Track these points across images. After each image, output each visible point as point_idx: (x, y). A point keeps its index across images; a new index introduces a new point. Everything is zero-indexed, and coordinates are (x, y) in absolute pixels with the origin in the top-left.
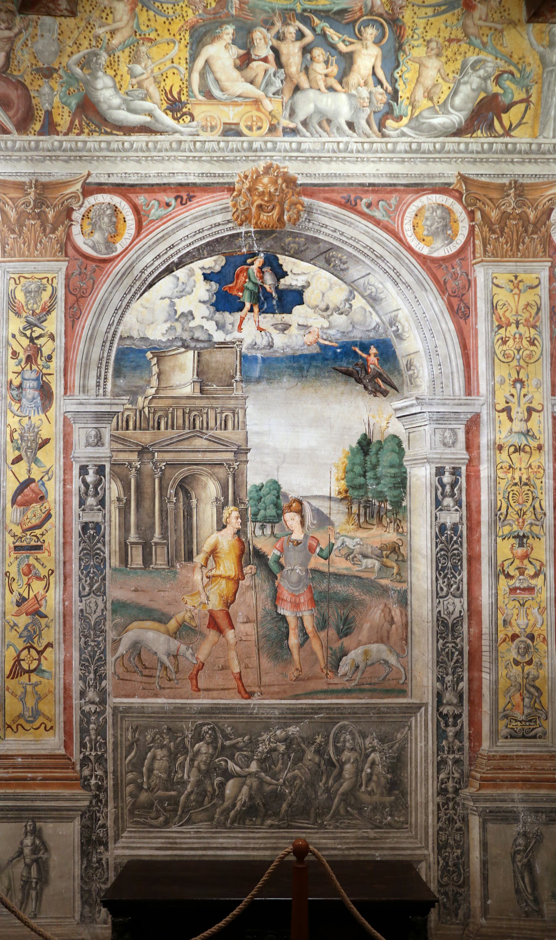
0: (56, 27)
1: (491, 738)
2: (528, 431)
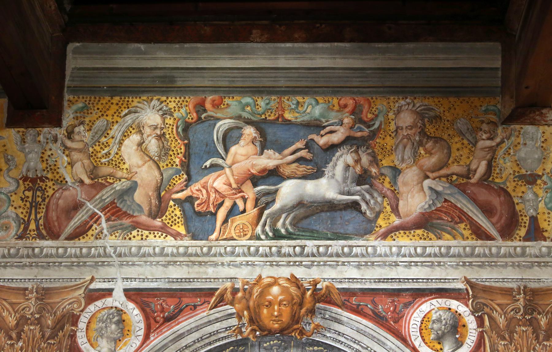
0: (539, 135)
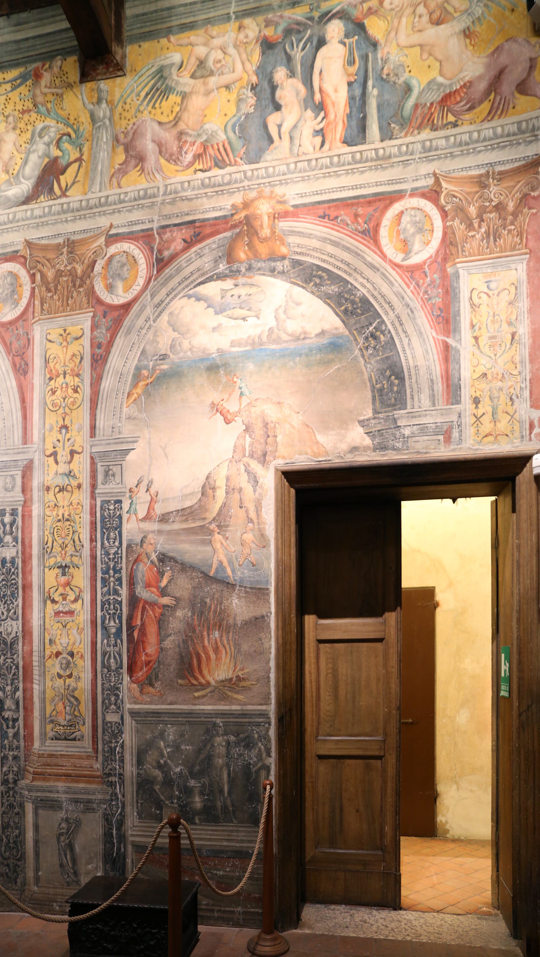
1: (41, 739)
2: (70, 472)
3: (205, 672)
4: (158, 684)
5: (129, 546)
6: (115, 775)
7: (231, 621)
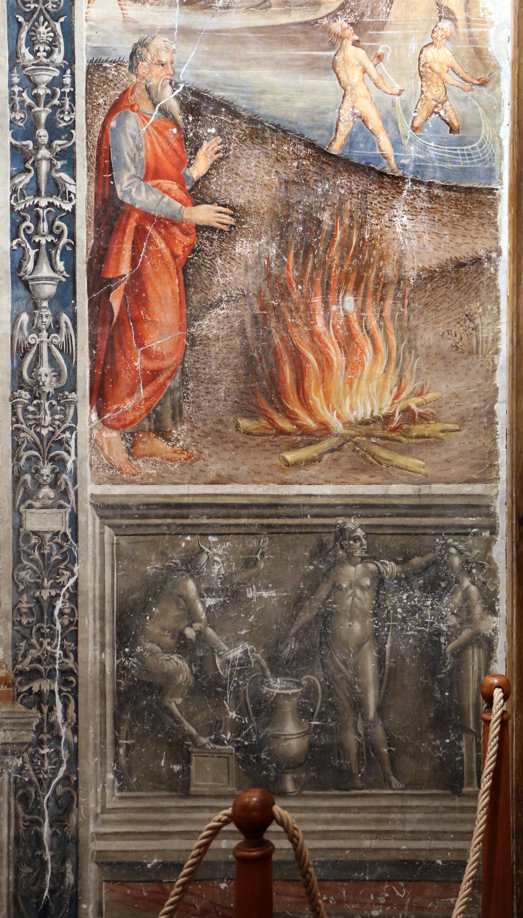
3: (317, 399)
4: (180, 432)
5: (95, 67)
6: (51, 675)
7: (390, 271)
